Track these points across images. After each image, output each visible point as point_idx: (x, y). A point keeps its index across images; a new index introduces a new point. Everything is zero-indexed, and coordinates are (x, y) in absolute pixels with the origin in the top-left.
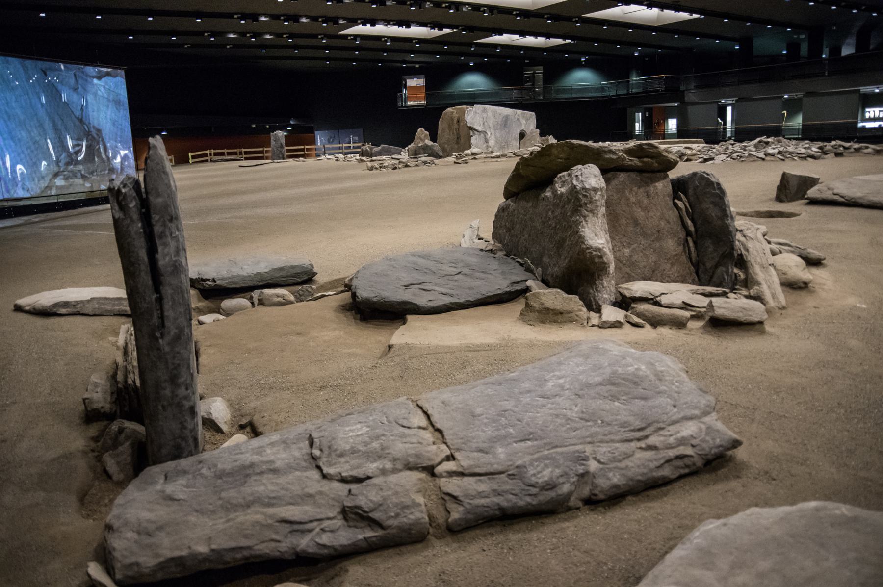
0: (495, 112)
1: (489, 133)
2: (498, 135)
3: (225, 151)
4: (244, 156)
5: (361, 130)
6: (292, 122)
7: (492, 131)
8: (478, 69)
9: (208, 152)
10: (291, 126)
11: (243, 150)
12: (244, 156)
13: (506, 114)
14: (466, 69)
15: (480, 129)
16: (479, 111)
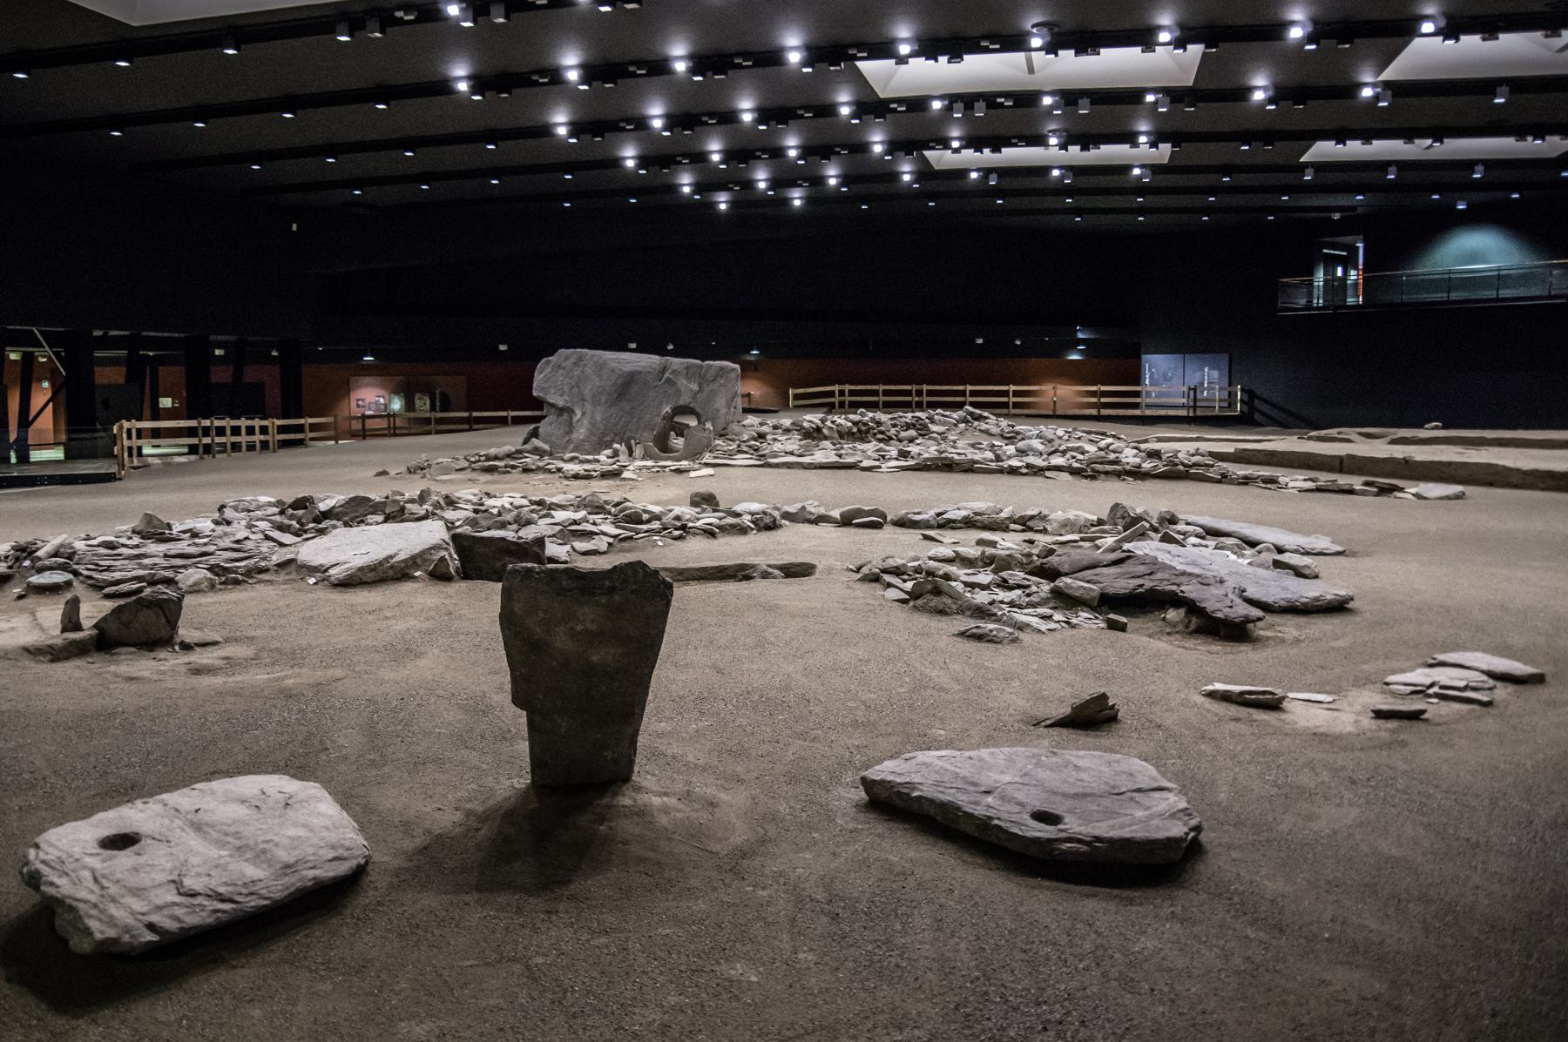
0: (602, 366)
1: (579, 413)
2: (598, 417)
3: (881, 388)
4: (926, 399)
5: (1226, 357)
6: (1080, 335)
7: (588, 407)
8: (1477, 218)
9: (836, 388)
10: (1083, 341)
11: (925, 387)
12: (926, 399)
13: (628, 368)
14: (1449, 222)
15: (560, 402)
16: (568, 363)
